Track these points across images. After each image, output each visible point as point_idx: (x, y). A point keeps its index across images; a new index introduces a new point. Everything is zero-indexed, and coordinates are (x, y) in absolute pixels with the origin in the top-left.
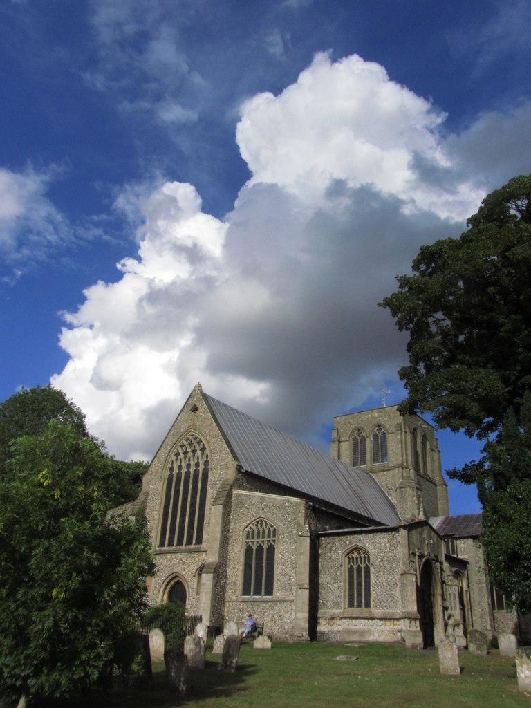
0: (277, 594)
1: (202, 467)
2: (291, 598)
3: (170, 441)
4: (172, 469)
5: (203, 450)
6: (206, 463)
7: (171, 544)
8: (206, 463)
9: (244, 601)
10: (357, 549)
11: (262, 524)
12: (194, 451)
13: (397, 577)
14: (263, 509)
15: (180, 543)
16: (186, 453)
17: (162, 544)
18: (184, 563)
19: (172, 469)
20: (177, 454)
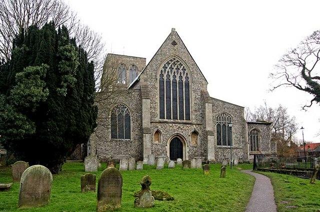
0: (234, 146)
1: (184, 80)
2: (241, 147)
3: (159, 58)
4: (162, 75)
5: (184, 69)
6: (187, 78)
7: (169, 118)
8: (187, 78)
9: (220, 148)
10: (254, 130)
11: (224, 115)
12: (178, 69)
13: (270, 141)
14: (224, 108)
15: (175, 118)
16: (171, 68)
17: (162, 117)
18: (182, 129)
19: (162, 75)
20: (165, 67)
